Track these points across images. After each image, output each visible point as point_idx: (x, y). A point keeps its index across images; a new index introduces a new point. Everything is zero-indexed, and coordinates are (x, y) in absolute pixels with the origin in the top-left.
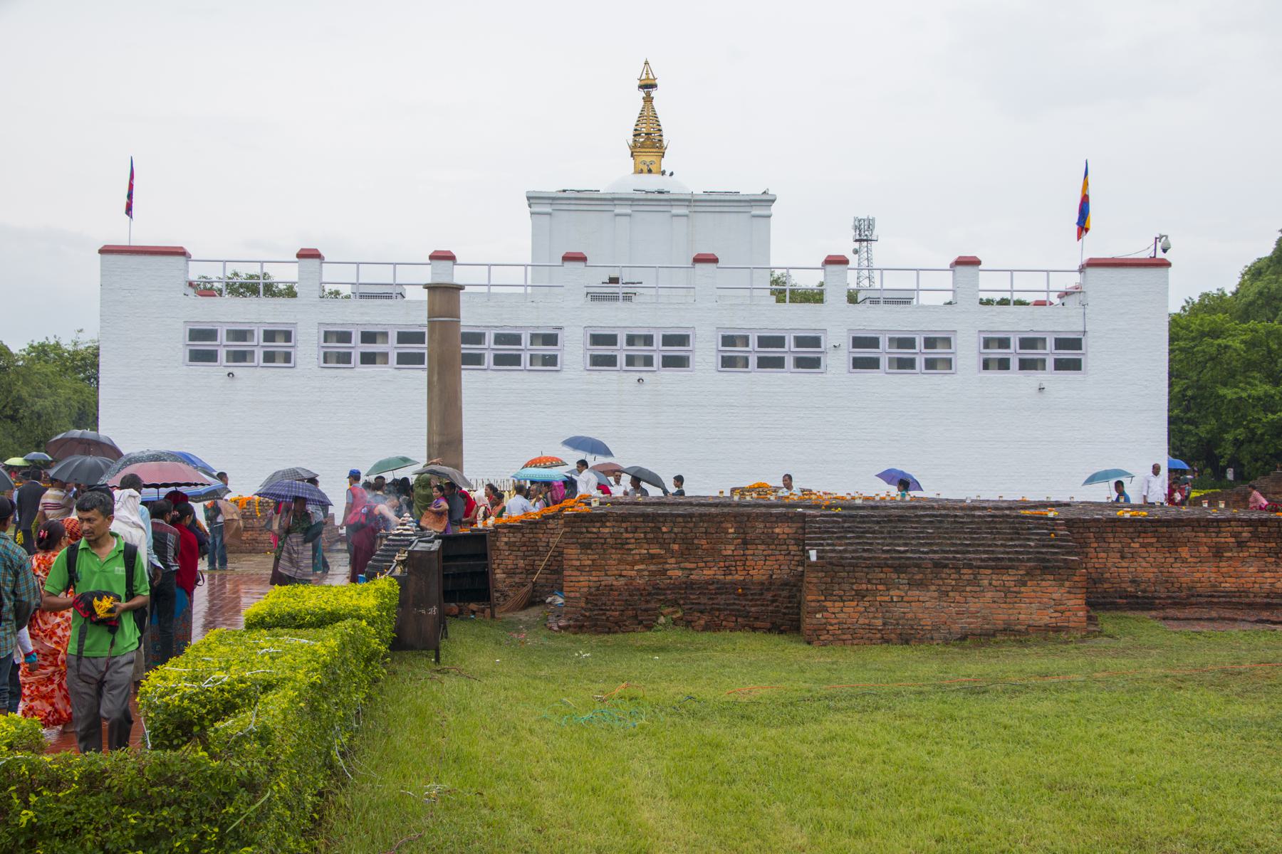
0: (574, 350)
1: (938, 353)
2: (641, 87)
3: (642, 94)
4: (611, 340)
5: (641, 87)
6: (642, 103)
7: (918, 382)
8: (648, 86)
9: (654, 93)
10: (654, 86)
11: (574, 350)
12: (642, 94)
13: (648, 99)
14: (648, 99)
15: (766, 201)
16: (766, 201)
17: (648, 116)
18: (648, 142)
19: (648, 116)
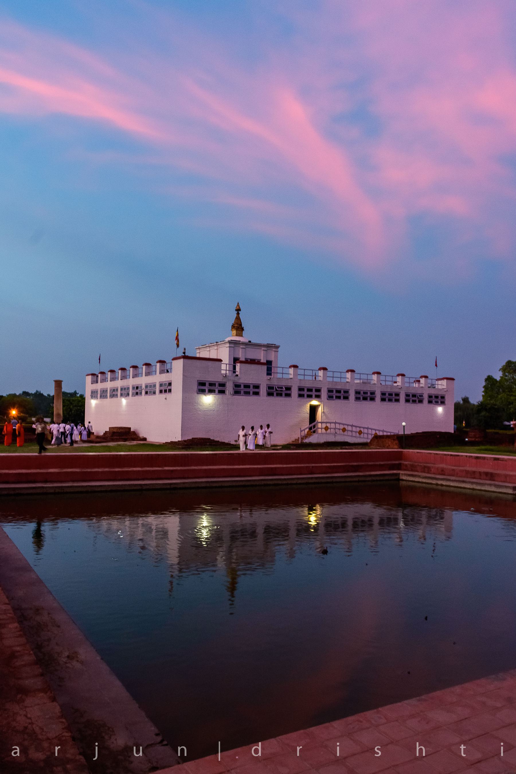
0: (263, 390)
1: (346, 395)
2: (236, 310)
3: (236, 312)
4: (272, 388)
5: (236, 310)
6: (236, 315)
7: (342, 402)
8: (238, 310)
9: (240, 312)
10: (240, 310)
11: (263, 390)
12: (236, 312)
13: (238, 314)
14: (238, 314)
15: (278, 347)
16: (278, 347)
17: (238, 318)
18: (238, 327)
19: (238, 318)
